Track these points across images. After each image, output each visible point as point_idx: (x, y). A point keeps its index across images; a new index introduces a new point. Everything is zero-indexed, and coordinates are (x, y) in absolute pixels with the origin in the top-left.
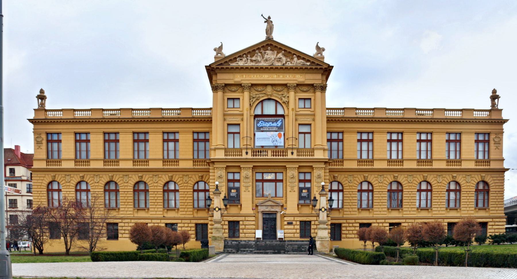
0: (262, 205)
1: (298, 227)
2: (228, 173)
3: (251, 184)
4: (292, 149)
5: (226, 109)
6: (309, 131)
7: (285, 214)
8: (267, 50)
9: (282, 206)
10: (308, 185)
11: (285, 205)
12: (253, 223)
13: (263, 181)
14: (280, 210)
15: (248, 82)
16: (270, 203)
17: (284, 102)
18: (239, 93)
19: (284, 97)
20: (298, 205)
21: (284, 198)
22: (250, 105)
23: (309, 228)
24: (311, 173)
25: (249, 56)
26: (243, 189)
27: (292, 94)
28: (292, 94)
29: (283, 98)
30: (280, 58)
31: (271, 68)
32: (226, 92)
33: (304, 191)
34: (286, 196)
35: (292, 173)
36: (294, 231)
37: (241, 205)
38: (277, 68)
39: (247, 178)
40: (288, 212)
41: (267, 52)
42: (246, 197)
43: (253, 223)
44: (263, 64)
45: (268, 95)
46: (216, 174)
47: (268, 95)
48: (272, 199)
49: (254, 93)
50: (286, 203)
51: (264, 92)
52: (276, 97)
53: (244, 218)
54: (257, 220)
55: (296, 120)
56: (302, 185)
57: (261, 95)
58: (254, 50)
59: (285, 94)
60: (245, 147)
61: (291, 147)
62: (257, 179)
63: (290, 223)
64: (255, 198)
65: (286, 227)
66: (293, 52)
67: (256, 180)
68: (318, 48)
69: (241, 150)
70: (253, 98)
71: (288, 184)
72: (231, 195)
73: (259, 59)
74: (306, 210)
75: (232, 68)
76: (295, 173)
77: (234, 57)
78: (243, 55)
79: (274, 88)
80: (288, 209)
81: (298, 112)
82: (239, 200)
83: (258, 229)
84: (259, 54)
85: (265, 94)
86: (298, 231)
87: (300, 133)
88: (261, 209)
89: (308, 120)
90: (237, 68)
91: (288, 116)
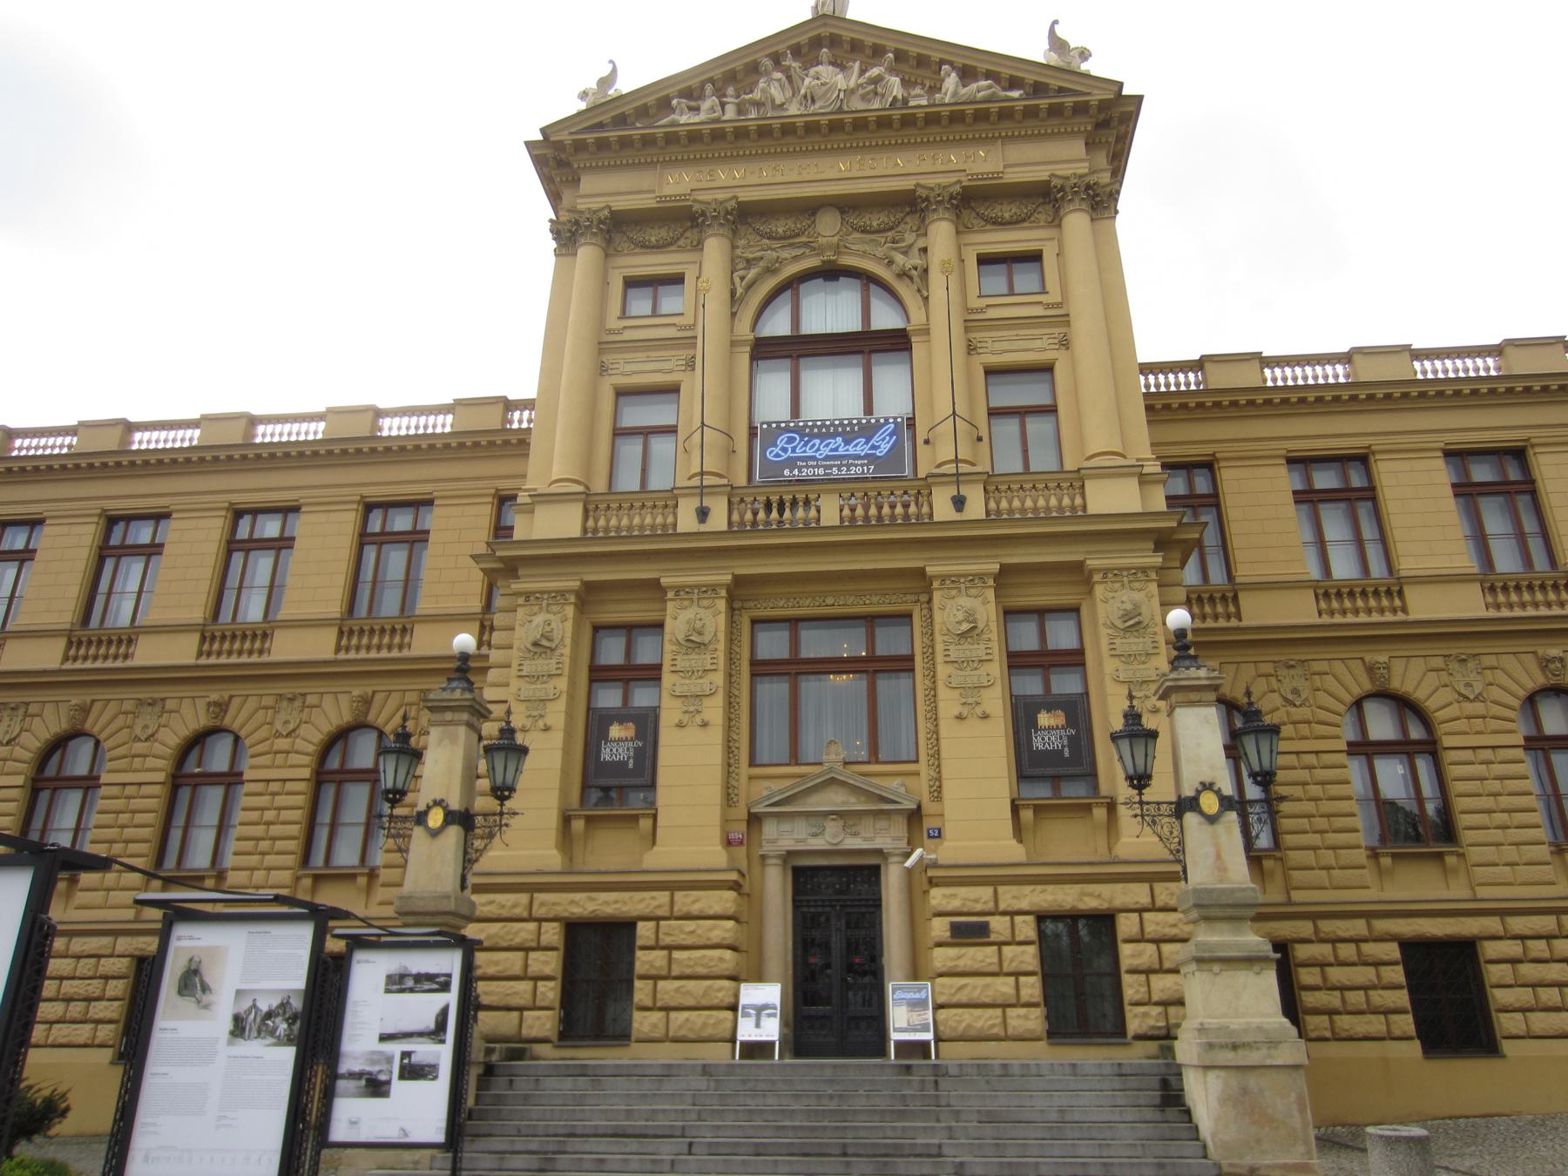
0: (785, 809)
1: (1028, 957)
2: (597, 629)
3: (719, 679)
4: (958, 478)
5: (613, 322)
6: (1047, 401)
7: (935, 865)
8: (819, 63)
9: (915, 816)
10: (1065, 684)
11: (929, 807)
12: (724, 930)
13: (795, 668)
14: (903, 844)
15: (721, 196)
16: (834, 799)
17: (903, 275)
18: (682, 250)
19: (905, 253)
20: (1015, 809)
21: (922, 767)
22: (733, 293)
23: (1102, 963)
24: (1075, 610)
25: (730, 91)
26: (670, 714)
27: (941, 233)
28: (941, 233)
29: (900, 259)
30: (876, 81)
31: (835, 127)
32: (618, 253)
33: (1044, 719)
34: (936, 755)
35: (963, 610)
36: (1004, 986)
37: (655, 817)
38: (860, 125)
39: (694, 645)
40: (951, 850)
41: (820, 68)
42: (691, 761)
43: (724, 930)
44: (793, 109)
45: (820, 250)
46: (519, 632)
47: (820, 250)
48: (844, 774)
49: (751, 246)
50: (937, 793)
51: (803, 239)
52: (864, 254)
53: (663, 897)
54: (748, 915)
55: (971, 349)
56: (1031, 685)
57: (786, 254)
58: (754, 69)
59: (909, 238)
60: (696, 482)
61: (950, 469)
62: (764, 653)
63: (969, 932)
64: (744, 770)
65: (942, 957)
66: (936, 56)
67: (754, 663)
68: (1057, 44)
69: (670, 499)
70: (750, 263)
71: (942, 671)
72: (606, 755)
73: (778, 95)
74: (1068, 842)
75: (648, 141)
76: (986, 608)
77: (657, 99)
78: (703, 84)
79: (853, 219)
80: (948, 831)
81: (981, 311)
82: (652, 785)
83: (759, 977)
84: (778, 75)
85: (806, 245)
86: (1032, 988)
87: (994, 413)
88: (783, 837)
89: (1038, 344)
90: (671, 139)
91: (926, 331)
